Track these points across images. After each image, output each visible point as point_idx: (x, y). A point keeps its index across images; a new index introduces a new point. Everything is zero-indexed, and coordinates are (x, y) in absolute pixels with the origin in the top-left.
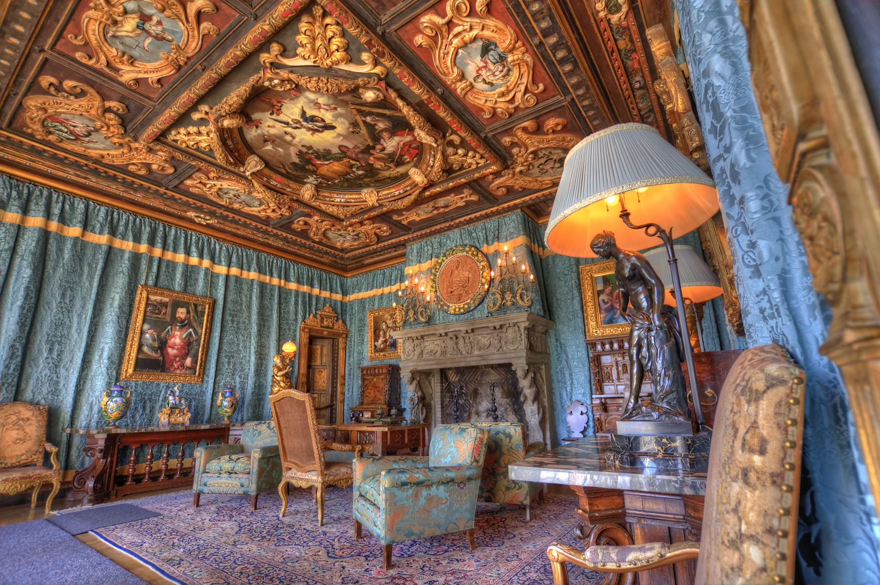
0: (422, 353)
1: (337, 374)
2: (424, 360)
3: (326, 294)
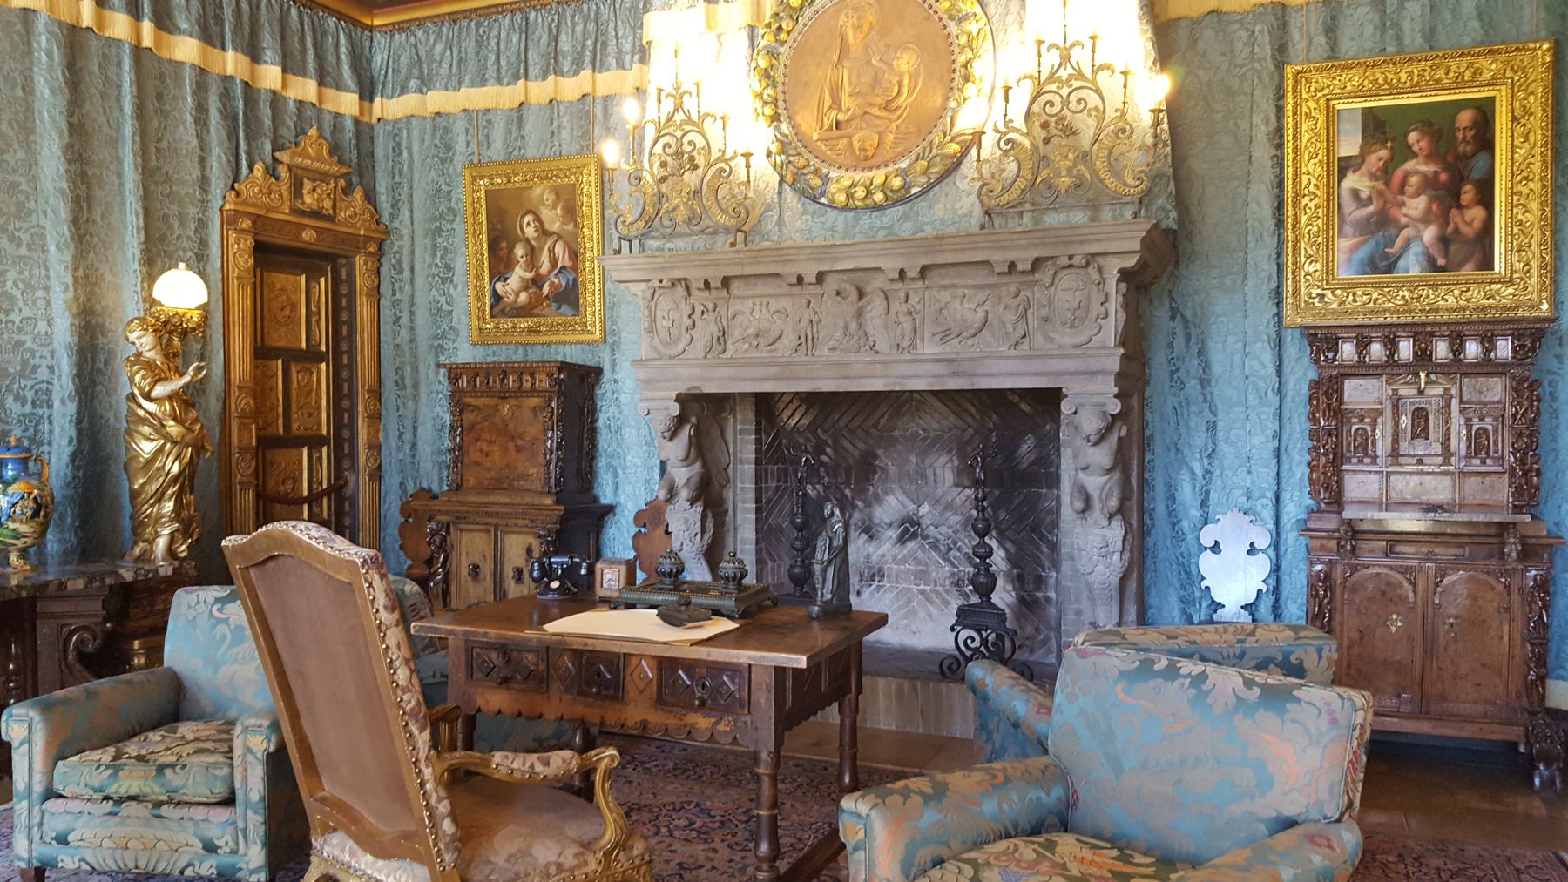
0: (722, 338)
1: (351, 380)
2: (732, 363)
3: (305, 89)
